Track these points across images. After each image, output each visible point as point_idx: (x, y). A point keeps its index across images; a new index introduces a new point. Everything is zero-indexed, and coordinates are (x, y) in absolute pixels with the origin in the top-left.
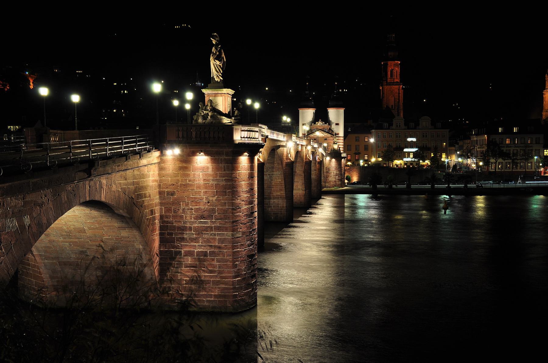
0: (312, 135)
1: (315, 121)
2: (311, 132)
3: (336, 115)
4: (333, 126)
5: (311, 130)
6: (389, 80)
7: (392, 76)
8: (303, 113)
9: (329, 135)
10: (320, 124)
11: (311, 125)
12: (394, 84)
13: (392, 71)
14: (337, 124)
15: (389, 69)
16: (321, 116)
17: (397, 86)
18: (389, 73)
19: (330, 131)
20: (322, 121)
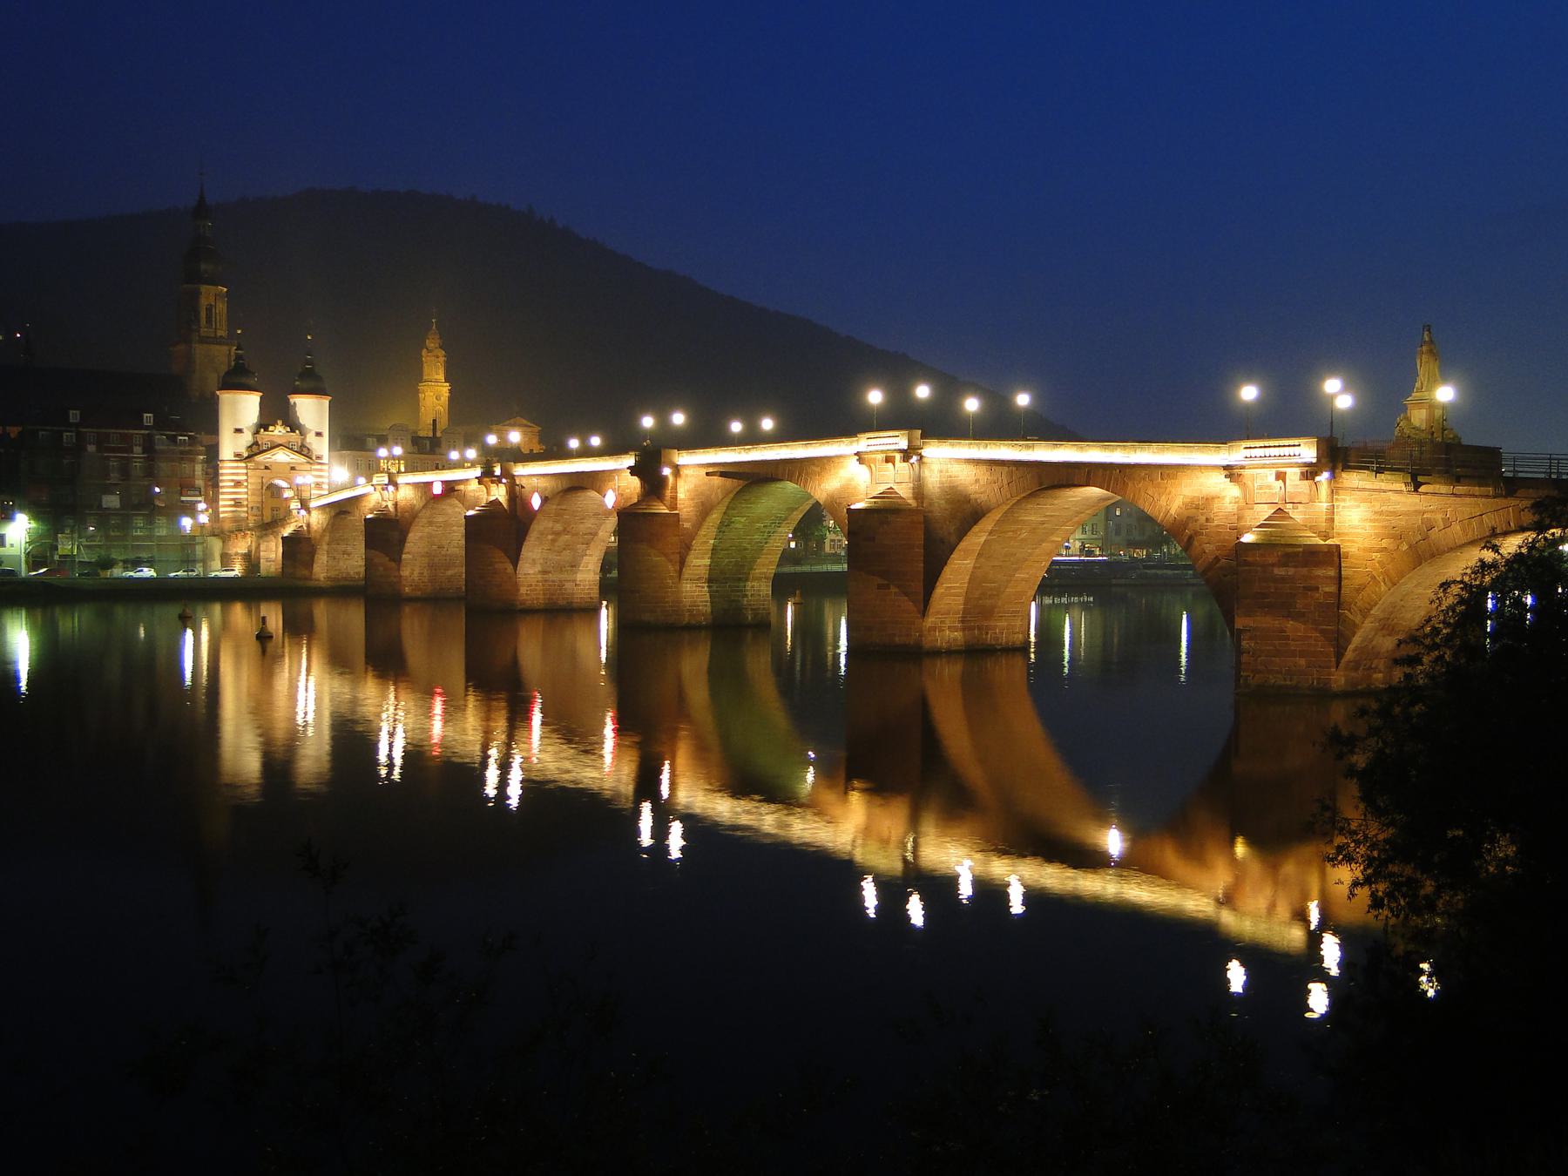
0: (259, 458)
1: (263, 425)
2: (255, 449)
3: (311, 410)
4: (311, 439)
5: (256, 443)
6: (204, 331)
7: (209, 320)
8: (234, 404)
9: (302, 459)
10: (278, 431)
11: (257, 432)
12: (217, 341)
13: (209, 309)
14: (319, 434)
15: (204, 302)
16: (276, 412)
17: (225, 348)
18: (203, 314)
19: (303, 450)
20: (285, 424)
